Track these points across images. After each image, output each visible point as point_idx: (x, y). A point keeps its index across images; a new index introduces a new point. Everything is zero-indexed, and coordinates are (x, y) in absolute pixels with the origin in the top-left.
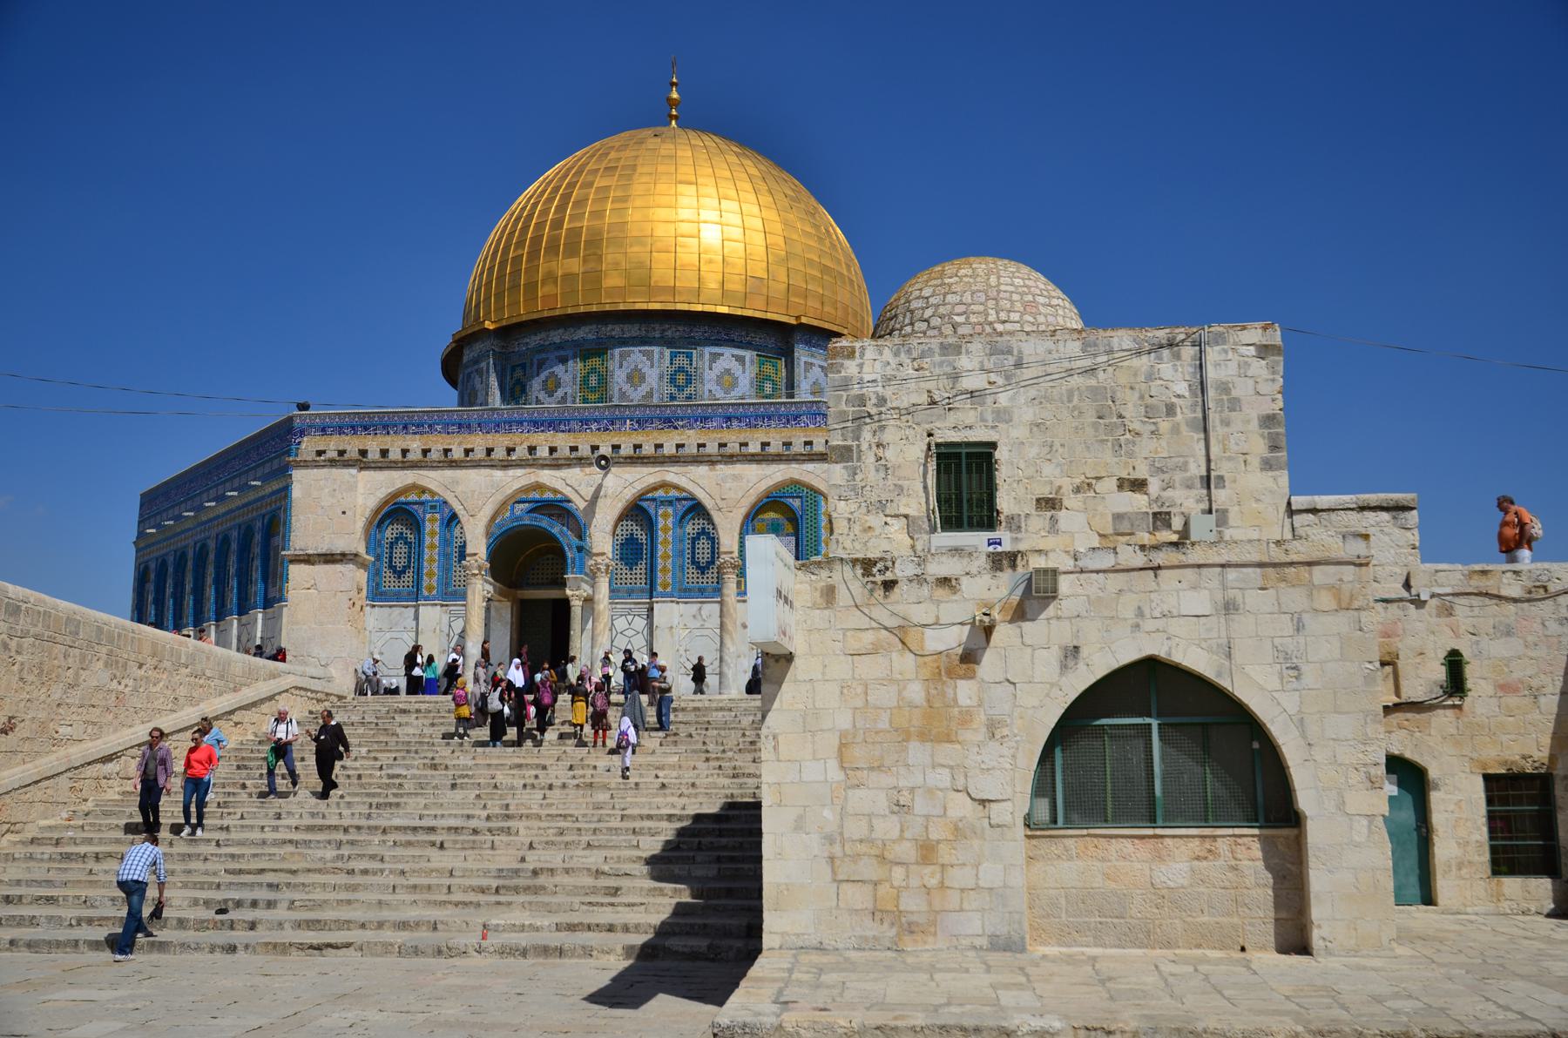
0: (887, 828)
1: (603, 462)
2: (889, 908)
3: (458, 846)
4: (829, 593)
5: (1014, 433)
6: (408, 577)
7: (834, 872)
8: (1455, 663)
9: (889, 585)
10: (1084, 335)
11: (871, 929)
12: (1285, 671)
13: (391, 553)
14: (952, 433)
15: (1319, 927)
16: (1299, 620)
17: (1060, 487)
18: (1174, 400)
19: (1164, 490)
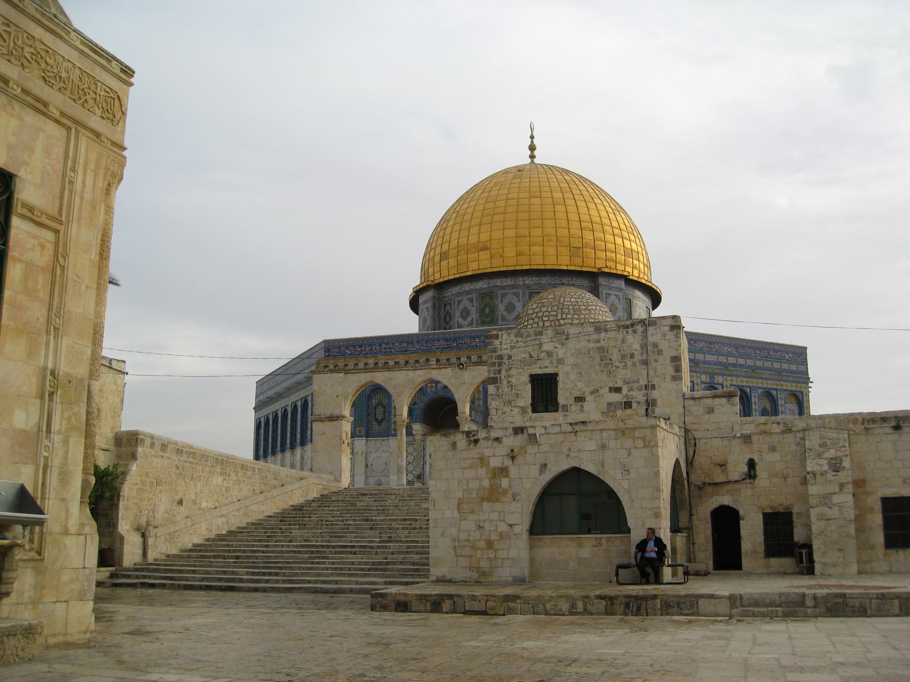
0: (476, 535)
1: (461, 366)
2: (476, 565)
3: (362, 553)
4: (454, 445)
5: (565, 369)
6: (384, 424)
7: (456, 552)
8: (751, 464)
9: (476, 441)
10: (595, 324)
12: (624, 472)
13: (375, 412)
16: (630, 451)
17: (584, 392)
18: (633, 352)
19: (629, 391)
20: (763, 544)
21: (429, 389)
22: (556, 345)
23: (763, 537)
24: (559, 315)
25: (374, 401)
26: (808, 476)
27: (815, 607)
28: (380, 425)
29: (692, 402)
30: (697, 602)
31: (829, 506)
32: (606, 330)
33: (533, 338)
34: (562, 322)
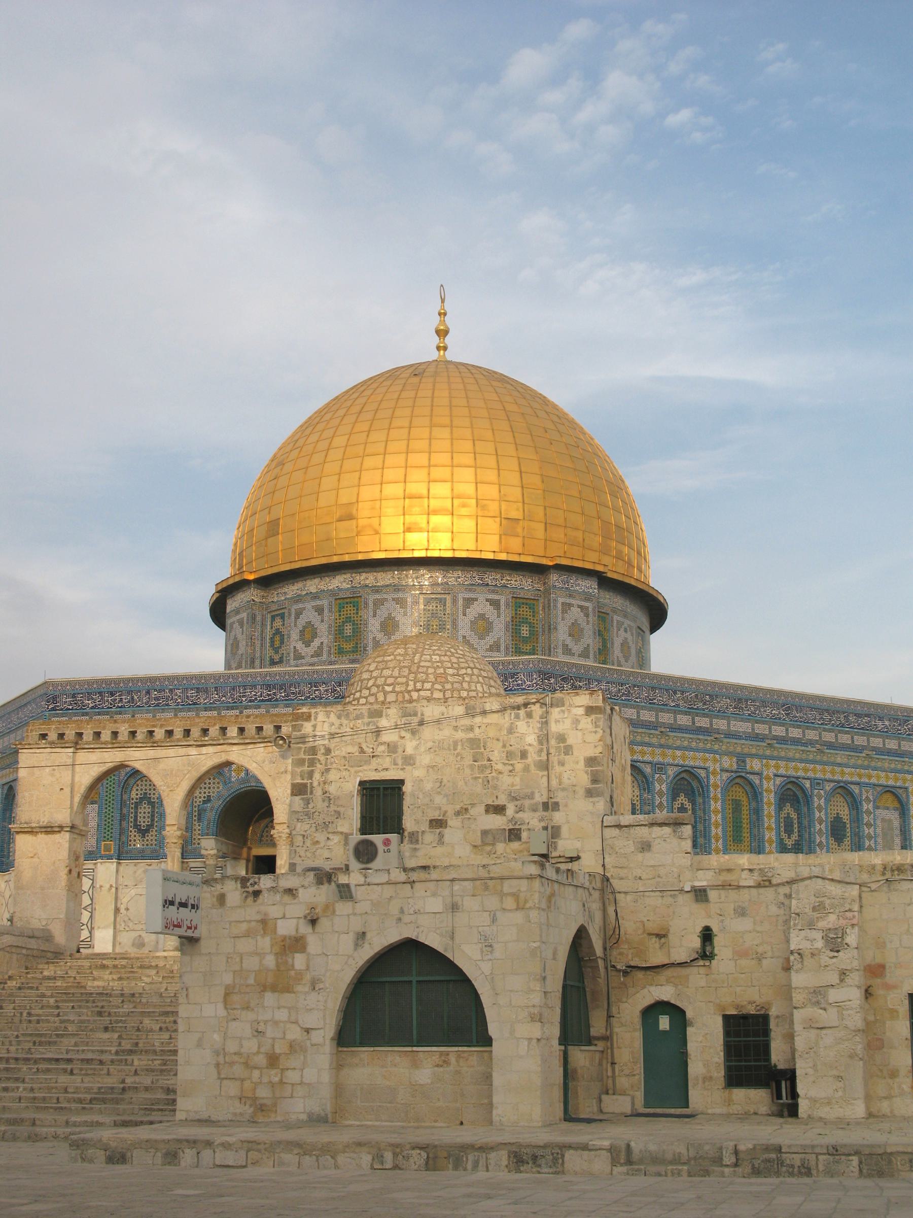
1: (281, 742)
2: (250, 1095)
6: (152, 836)
7: (219, 1073)
8: (707, 935)
9: (257, 894)
10: (467, 701)
11: (238, 1108)
12: (484, 949)
13: (136, 813)
14: (374, 773)
15: (497, 1108)
16: (495, 915)
17: (446, 812)
18: (526, 747)
19: (517, 812)
20: (722, 1067)
21: (233, 773)
22: (403, 733)
23: (722, 1054)
24: (411, 683)
25: (134, 793)
26: (792, 958)
27: (736, 1165)
28: (144, 836)
29: (615, 832)
30: (563, 1156)
31: (822, 1006)
32: (484, 713)
33: (366, 720)
34: (415, 695)
